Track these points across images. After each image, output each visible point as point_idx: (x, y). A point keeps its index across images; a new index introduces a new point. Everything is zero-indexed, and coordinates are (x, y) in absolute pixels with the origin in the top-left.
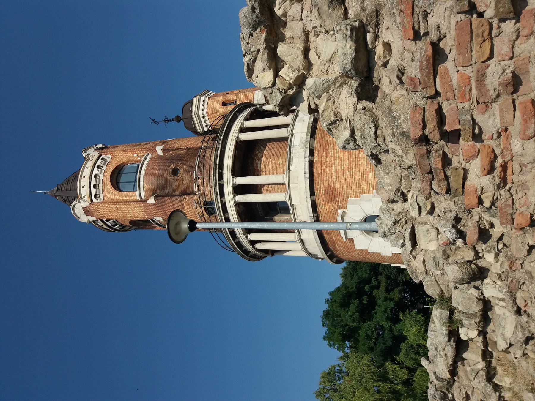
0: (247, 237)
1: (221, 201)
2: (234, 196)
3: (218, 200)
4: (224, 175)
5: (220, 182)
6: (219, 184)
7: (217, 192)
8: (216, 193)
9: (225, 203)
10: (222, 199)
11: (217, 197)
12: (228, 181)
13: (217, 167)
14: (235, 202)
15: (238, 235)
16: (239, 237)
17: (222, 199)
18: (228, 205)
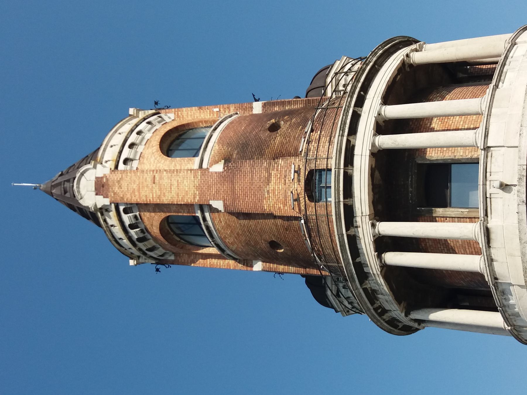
0: (373, 226)
1: (348, 141)
2: (375, 135)
3: (342, 136)
4: (366, 101)
5: (357, 109)
6: (354, 112)
7: (345, 123)
8: (344, 123)
9: (353, 147)
10: (351, 138)
11: (343, 131)
12: (373, 107)
13: (360, 85)
14: (373, 145)
15: (358, 219)
16: (359, 223)
17: (351, 138)
18: (357, 151)
